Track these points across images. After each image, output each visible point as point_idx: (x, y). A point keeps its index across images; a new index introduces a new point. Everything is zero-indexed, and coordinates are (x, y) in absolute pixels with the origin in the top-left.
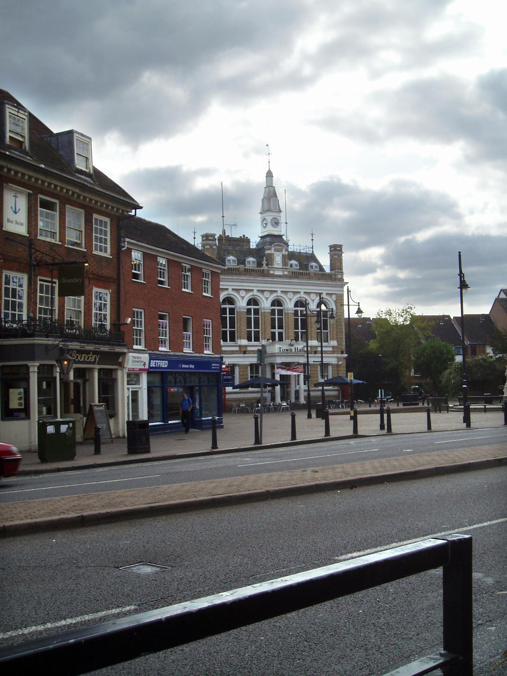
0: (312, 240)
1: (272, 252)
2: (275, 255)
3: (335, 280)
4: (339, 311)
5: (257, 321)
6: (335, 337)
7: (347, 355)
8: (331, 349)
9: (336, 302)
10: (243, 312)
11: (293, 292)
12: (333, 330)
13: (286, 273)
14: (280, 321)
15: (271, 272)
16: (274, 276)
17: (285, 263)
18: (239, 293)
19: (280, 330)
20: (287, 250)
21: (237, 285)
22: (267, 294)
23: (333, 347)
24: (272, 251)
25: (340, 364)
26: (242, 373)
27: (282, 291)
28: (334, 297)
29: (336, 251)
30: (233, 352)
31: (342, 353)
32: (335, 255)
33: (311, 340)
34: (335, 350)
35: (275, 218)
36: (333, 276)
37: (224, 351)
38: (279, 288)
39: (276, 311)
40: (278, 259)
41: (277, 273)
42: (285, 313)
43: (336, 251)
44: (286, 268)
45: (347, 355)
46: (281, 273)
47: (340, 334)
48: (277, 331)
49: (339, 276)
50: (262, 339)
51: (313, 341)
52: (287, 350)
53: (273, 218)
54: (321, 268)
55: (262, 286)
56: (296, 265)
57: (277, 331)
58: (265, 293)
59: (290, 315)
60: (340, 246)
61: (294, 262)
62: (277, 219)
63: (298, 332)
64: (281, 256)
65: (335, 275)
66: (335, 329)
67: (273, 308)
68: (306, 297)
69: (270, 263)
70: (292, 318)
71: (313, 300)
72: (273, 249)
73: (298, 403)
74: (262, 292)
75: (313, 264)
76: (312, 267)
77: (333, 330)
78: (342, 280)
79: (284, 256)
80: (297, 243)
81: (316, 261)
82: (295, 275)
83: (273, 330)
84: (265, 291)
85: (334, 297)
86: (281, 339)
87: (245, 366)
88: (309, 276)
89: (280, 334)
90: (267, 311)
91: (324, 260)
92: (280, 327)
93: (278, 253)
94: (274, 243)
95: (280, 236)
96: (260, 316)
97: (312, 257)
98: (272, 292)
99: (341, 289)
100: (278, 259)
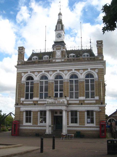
2: (57, 52)
5: (32, 88)
6: (98, 94)
8: (95, 102)
9: (98, 73)
10: (36, 83)
11: (68, 70)
13: (63, 60)
15: (54, 61)
16: (55, 62)
21: (33, 69)
23: (96, 100)
24: (55, 50)
26: (83, 116)
28: (97, 71)
30: (29, 104)
33: (80, 96)
35: (59, 34)
37: (25, 104)
38: (58, 69)
40: (58, 53)
41: (57, 61)
44: (63, 58)
46: (60, 61)
49: (100, 58)
53: (58, 34)
56: (74, 56)
57: (59, 92)
58: (50, 72)
64: (60, 51)
72: (55, 49)
79: (62, 52)
85: (97, 71)
87: (36, 112)
90: (51, 82)
92: (60, 91)
93: (59, 50)
96: (39, 85)
98: (54, 71)
100: (58, 53)
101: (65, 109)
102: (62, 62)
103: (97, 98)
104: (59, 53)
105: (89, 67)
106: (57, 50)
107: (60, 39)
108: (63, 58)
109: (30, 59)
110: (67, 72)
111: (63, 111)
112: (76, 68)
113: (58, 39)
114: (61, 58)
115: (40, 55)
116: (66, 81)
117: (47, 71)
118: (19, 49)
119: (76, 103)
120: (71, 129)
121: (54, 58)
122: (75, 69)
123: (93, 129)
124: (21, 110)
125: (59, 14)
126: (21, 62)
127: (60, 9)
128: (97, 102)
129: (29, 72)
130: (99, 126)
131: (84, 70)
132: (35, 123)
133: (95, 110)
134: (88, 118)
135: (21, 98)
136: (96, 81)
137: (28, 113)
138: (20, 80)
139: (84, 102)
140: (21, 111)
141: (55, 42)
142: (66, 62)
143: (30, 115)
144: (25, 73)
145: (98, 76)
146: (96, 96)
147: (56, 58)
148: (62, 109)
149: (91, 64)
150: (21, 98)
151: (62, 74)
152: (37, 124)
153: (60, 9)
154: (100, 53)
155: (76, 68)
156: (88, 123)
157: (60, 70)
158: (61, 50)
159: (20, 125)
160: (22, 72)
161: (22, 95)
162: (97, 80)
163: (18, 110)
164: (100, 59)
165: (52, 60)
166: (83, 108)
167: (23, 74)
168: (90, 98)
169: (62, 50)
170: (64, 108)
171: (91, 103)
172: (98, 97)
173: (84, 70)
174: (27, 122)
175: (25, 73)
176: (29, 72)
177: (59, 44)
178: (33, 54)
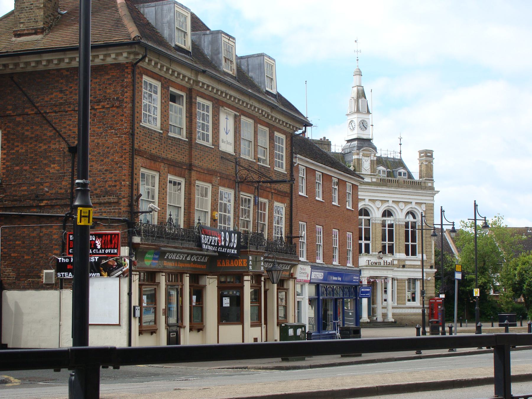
0: (400, 144)
1: (360, 158)
2: (364, 160)
3: (426, 188)
7: (436, 270)
11: (381, 200)
13: (374, 180)
14: (367, 231)
17: (373, 170)
19: (367, 242)
20: (375, 156)
24: (361, 157)
25: (429, 279)
27: (393, 201)
29: (427, 156)
31: (431, 267)
33: (399, 252)
35: (363, 120)
36: (423, 184)
39: (363, 220)
40: (366, 166)
42: (373, 223)
43: (427, 156)
44: (374, 175)
45: (436, 270)
47: (429, 247)
48: (363, 242)
49: (430, 185)
50: (396, 252)
51: (401, 254)
52: (376, 263)
54: (410, 176)
57: (363, 242)
59: (377, 226)
60: (431, 152)
61: (381, 168)
63: (409, 245)
64: (369, 161)
65: (425, 182)
67: (384, 218)
68: (394, 205)
70: (379, 229)
71: (402, 210)
72: (361, 153)
73: (386, 320)
75: (402, 171)
76: (400, 174)
78: (432, 188)
79: (372, 162)
80: (385, 148)
81: (405, 167)
82: (383, 183)
83: (360, 242)
85: (424, 207)
86: (367, 251)
88: (398, 184)
89: (367, 246)
91: (414, 167)
92: (367, 239)
93: (366, 158)
94: (362, 147)
95: (369, 140)
97: (400, 163)
99: (432, 198)
101: (391, 276)
105: (414, 199)
106: (363, 158)
107: (365, 132)
108: (374, 175)
110: (380, 204)
113: (362, 132)
114: (371, 175)
131: (406, 203)
134: (408, 291)
147: (363, 173)
149: (417, 194)
156: (409, 300)
169: (372, 159)
171: (414, 265)
173: (406, 203)
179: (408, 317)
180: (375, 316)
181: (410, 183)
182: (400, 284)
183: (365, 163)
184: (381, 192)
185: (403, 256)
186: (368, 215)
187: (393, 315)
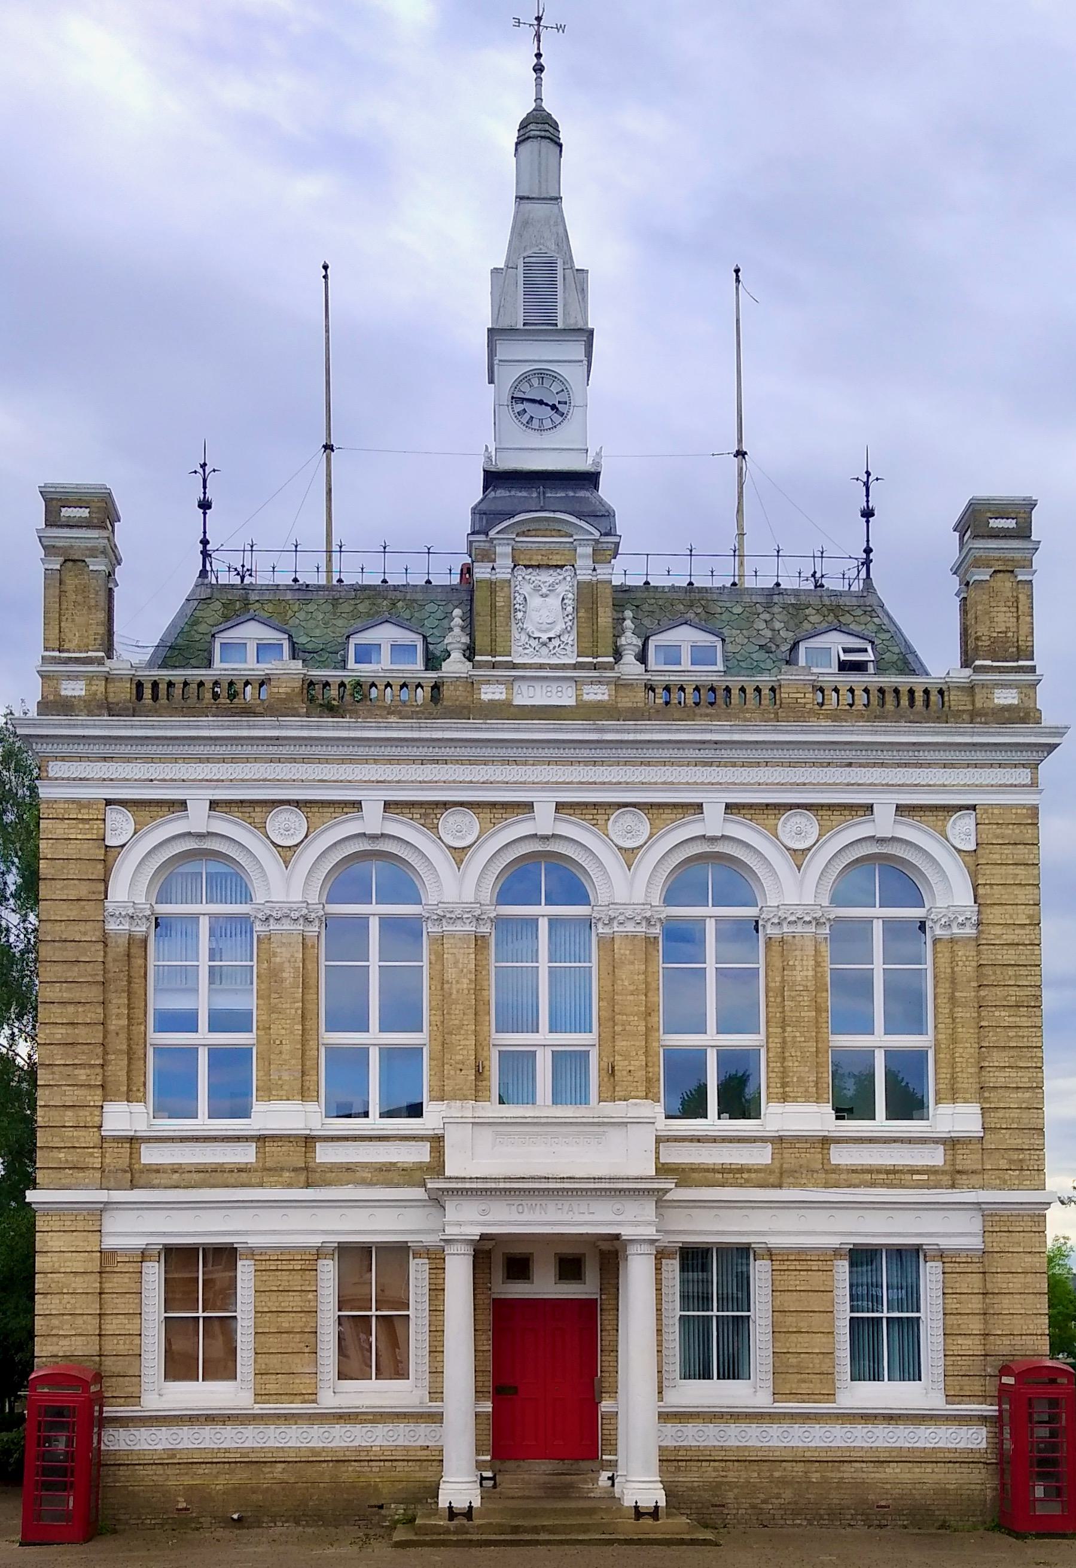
2: (526, 589)
4: (994, 915)
6: (967, 1080)
8: (935, 1157)
9: (974, 862)
12: (954, 1040)
13: (597, 694)
15: (490, 693)
18: (262, 828)
22: (458, 828)
23: (952, 1143)
24: (503, 572)
28: (963, 831)
32: (978, 563)
33: (784, 1098)
34: (968, 1160)
36: (955, 699)
37: (157, 1169)
38: (544, 785)
41: (528, 696)
44: (595, 667)
46: (566, 697)
49: (1006, 698)
55: (419, 781)
62: (555, 377)
65: (970, 689)
66: (966, 1033)
69: (481, 641)
72: (503, 550)
74: (427, 812)
77: (954, 1040)
79: (587, 596)
82: (670, 700)
84: (446, 805)
87: (293, 1264)
93: (546, 577)
99: (1023, 776)
100: (543, 612)
101: (650, 1232)
102: (585, 711)
103: (954, 1118)
104: (554, 602)
106: (521, 572)
108: (595, 667)
109: (184, 647)
110: (645, 829)
111: (632, 1249)
112: (745, 787)
113: (534, 440)
114: (576, 666)
115: (326, 612)
116: (630, 927)
117: (412, 804)
118: (52, 520)
119: (741, 1170)
120: (693, 1436)
121: (494, 666)
122: (729, 807)
123: (927, 1438)
124: (109, 1243)
125: (523, 126)
126: (90, 678)
127: (539, 69)
128: (961, 1160)
129: (198, 801)
130: (990, 1409)
132: (283, 1379)
133: (944, 1243)
135: (108, 1107)
136: (952, 940)
137: (198, 1271)
138: (83, 890)
139: (826, 1159)
140: (114, 1252)
141: (493, 479)
142: (635, 714)
143: (224, 1294)
144: (145, 809)
145: (975, 887)
146: (952, 1094)
148: (626, 1232)
150: (108, 1107)
151: (592, 847)
152: (312, 1397)
153: (539, 69)
154: (996, 642)
155: (745, 787)
157: (560, 806)
158: (567, 573)
159: (109, 1411)
160: (109, 802)
161: (118, 1067)
162: (970, 931)
163: (80, 1242)
164: (1008, 708)
165: (471, 684)
166: (818, 1221)
167: (120, 826)
168: (881, 1124)
169: (584, 576)
170: (635, 1222)
171: (893, 1171)
172: (975, 1109)
174: (179, 1367)
175: (145, 809)
176: (198, 801)
177: (538, 498)
178: (222, 603)
179: (848, 1472)
180: (613, 1465)
181: (892, 693)
182: (792, 1281)
183: (535, 601)
184: (640, 753)
185: (814, 1117)
186: (583, 899)
187: (670, 1460)
